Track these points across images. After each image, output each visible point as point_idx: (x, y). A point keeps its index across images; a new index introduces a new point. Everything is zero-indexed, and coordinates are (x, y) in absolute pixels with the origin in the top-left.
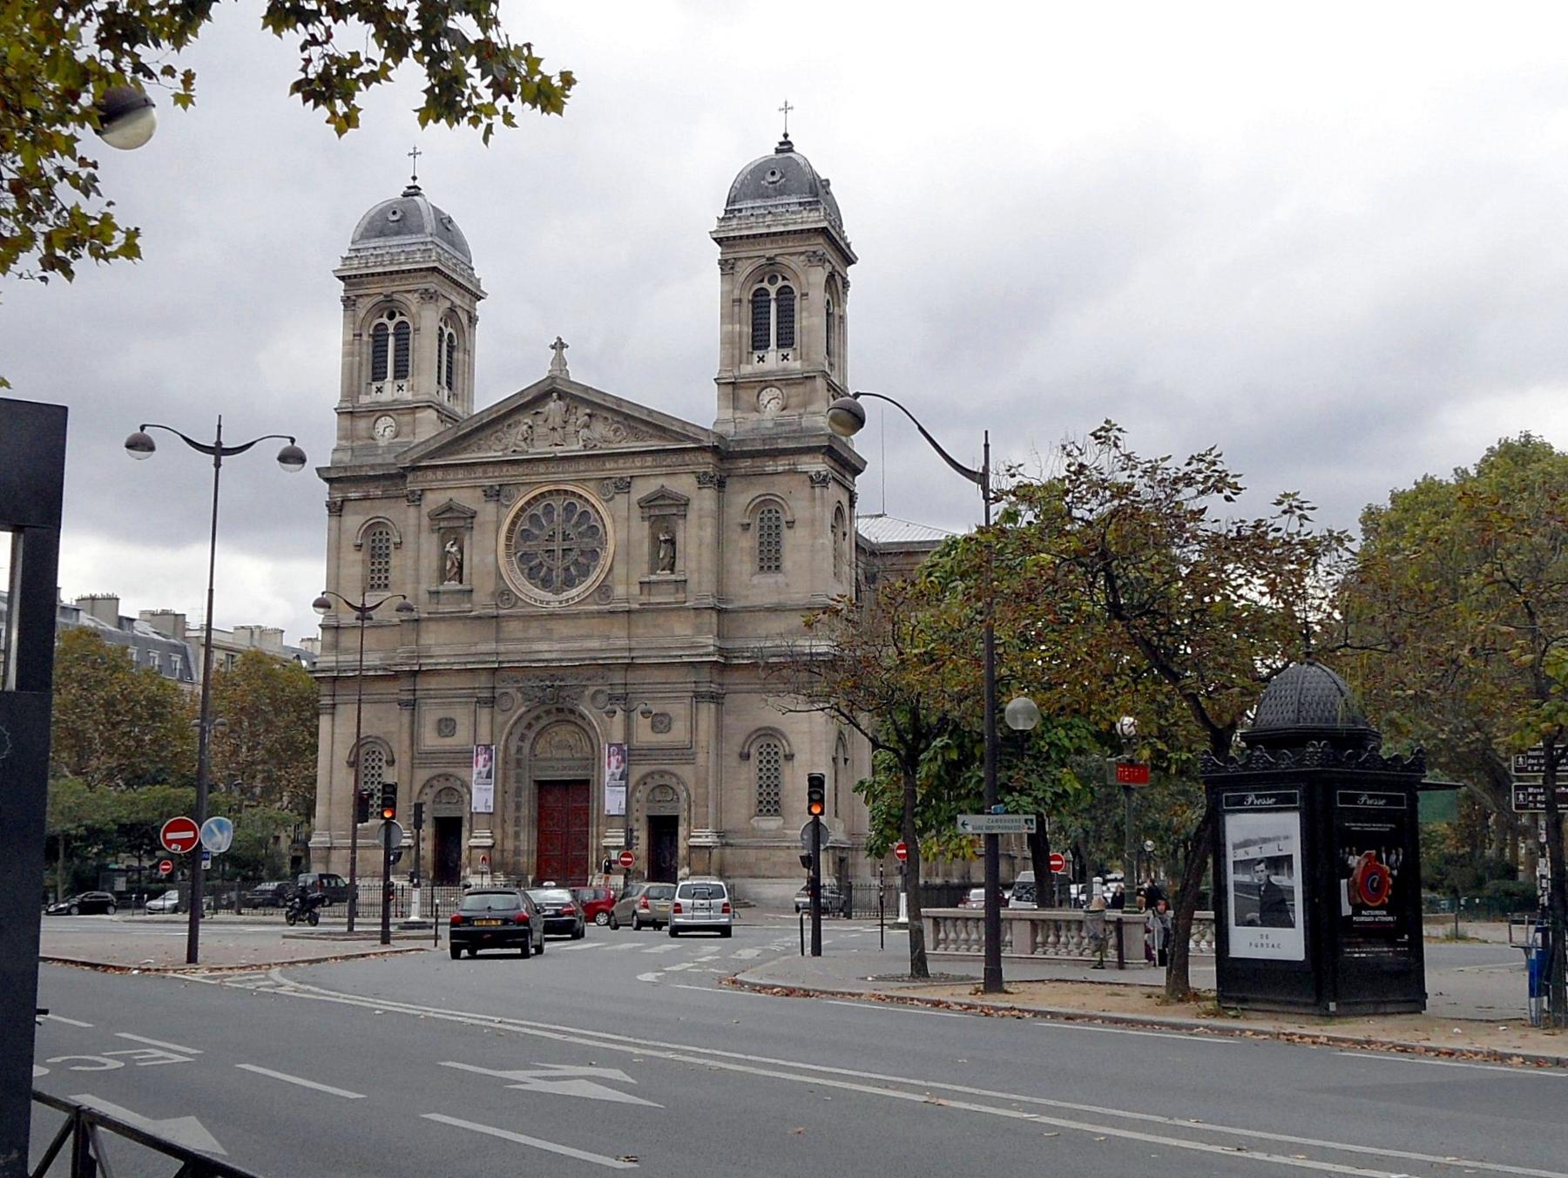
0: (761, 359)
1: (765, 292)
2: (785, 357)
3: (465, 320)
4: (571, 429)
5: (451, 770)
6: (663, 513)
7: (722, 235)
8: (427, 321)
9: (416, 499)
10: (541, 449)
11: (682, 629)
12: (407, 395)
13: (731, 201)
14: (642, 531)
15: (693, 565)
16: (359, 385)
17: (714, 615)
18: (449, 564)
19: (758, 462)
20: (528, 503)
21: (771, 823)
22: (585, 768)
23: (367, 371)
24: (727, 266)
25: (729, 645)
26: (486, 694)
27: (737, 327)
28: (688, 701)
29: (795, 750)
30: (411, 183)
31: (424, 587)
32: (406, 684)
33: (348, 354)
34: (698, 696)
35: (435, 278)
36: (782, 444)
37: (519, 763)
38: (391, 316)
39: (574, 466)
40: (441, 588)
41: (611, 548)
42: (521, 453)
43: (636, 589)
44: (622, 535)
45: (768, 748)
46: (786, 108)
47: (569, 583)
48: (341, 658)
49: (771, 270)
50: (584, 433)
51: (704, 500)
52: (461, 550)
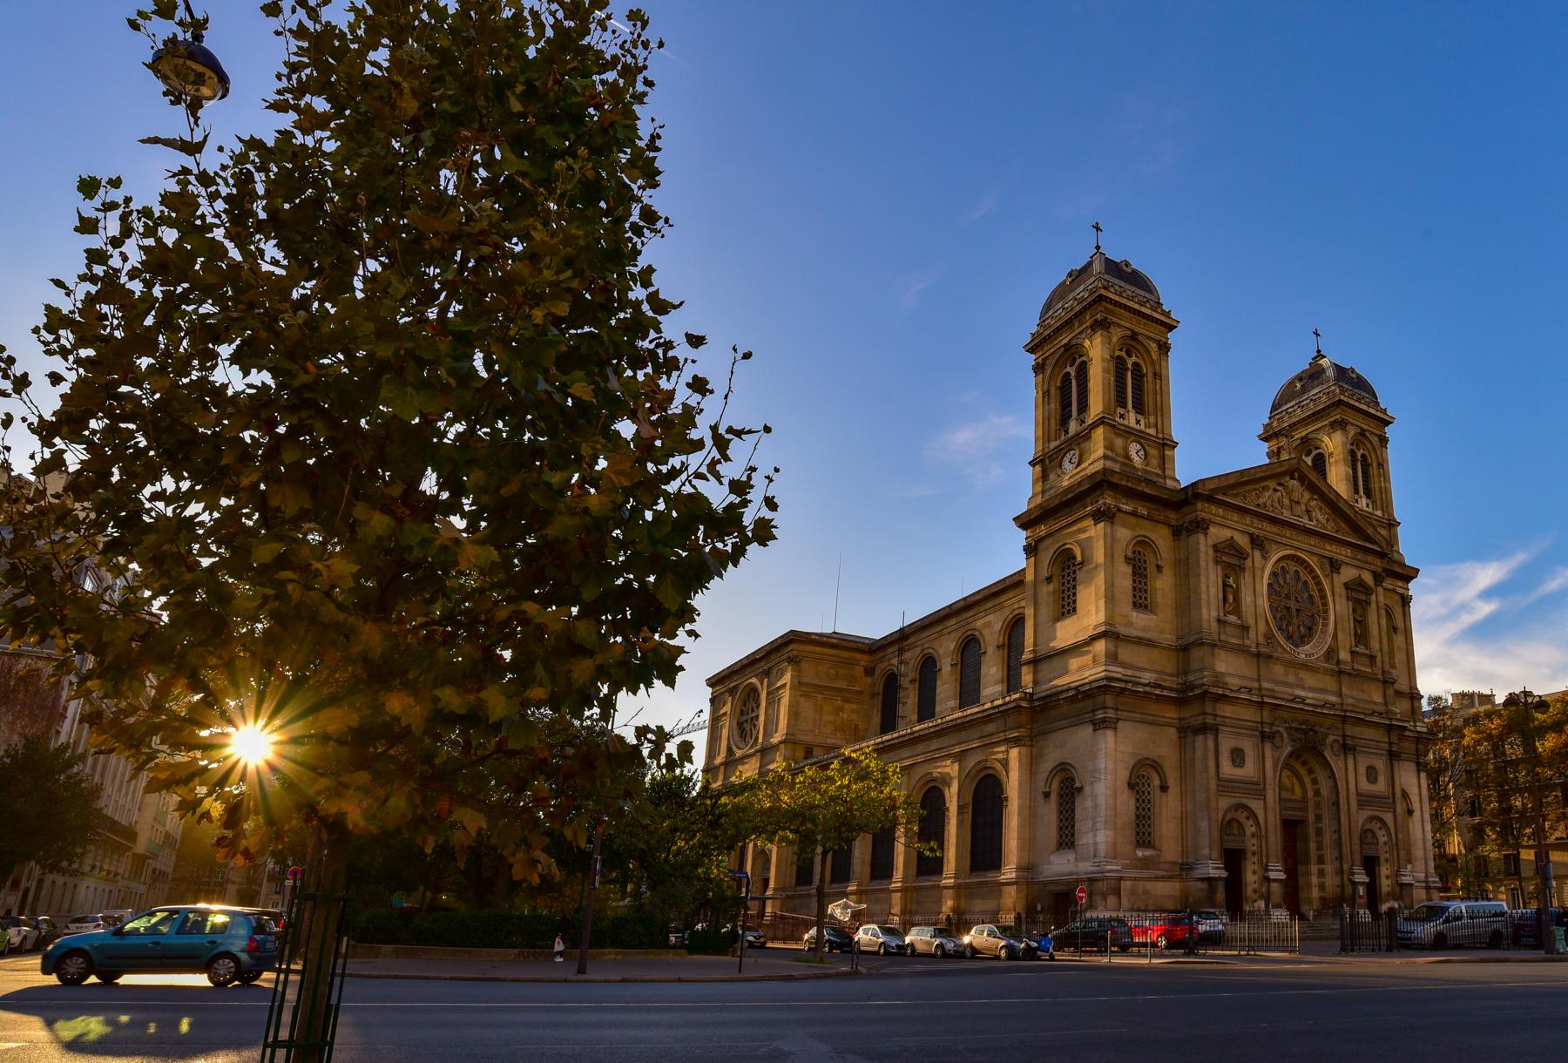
5: (1245, 801)
22: (1300, 810)
39: (1306, 539)
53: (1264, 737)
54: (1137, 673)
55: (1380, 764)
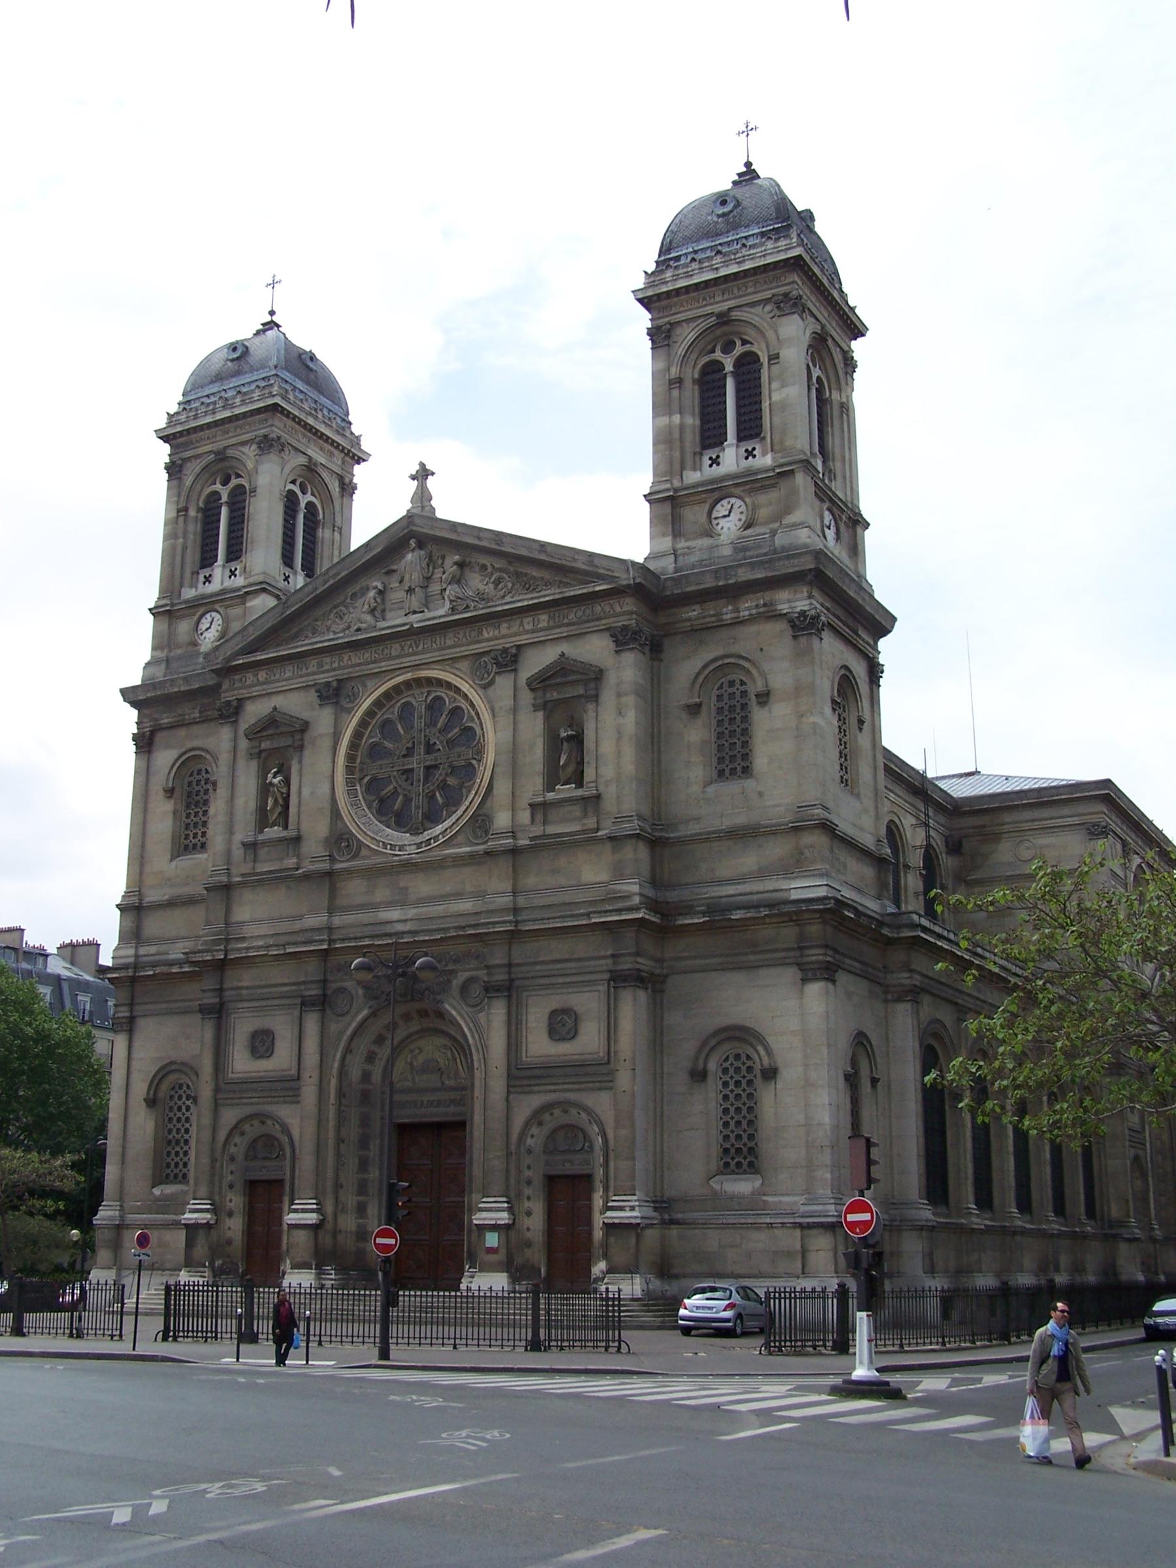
0: (715, 461)
1: (719, 366)
2: (750, 454)
3: (334, 486)
4: (435, 588)
5: (269, 1108)
6: (565, 695)
7: (650, 293)
8: (269, 479)
9: (231, 713)
10: (396, 620)
11: (593, 870)
12: (239, 581)
13: (665, 249)
14: (533, 726)
15: (608, 772)
16: (182, 578)
17: (643, 852)
18: (270, 802)
19: (711, 608)
20: (378, 703)
21: (743, 1186)
23: (193, 556)
24: (660, 336)
25: (673, 896)
26: (314, 991)
27: (677, 419)
28: (603, 988)
29: (780, 1063)
30: (268, 318)
31: (239, 837)
32: (210, 983)
33: (171, 536)
34: (618, 980)
35: (279, 421)
36: (744, 575)
37: (365, 1097)
38: (225, 482)
40: (261, 837)
41: (490, 757)
42: (366, 630)
43: (525, 816)
44: (506, 735)
45: (739, 1062)
46: (748, 130)
47: (433, 818)
48: (143, 951)
49: (724, 329)
50: (452, 591)
51: (626, 671)
52: (287, 782)
53: (306, 1004)
54: (163, 948)
55: (589, 1002)
